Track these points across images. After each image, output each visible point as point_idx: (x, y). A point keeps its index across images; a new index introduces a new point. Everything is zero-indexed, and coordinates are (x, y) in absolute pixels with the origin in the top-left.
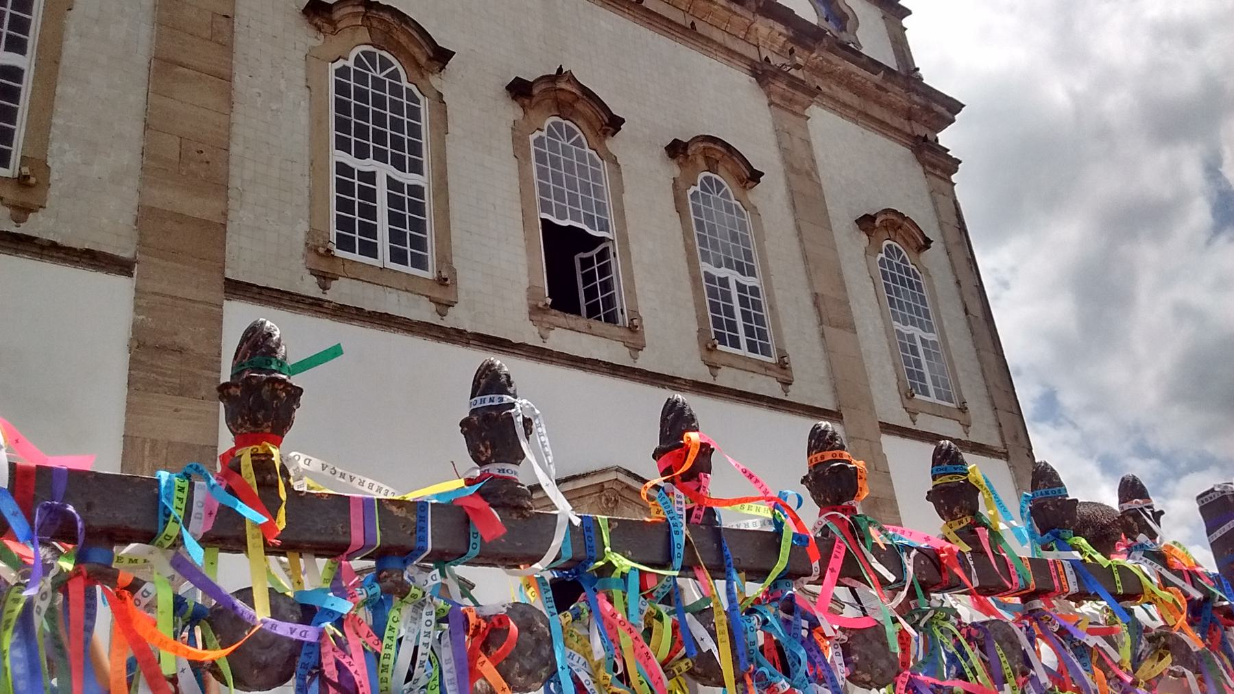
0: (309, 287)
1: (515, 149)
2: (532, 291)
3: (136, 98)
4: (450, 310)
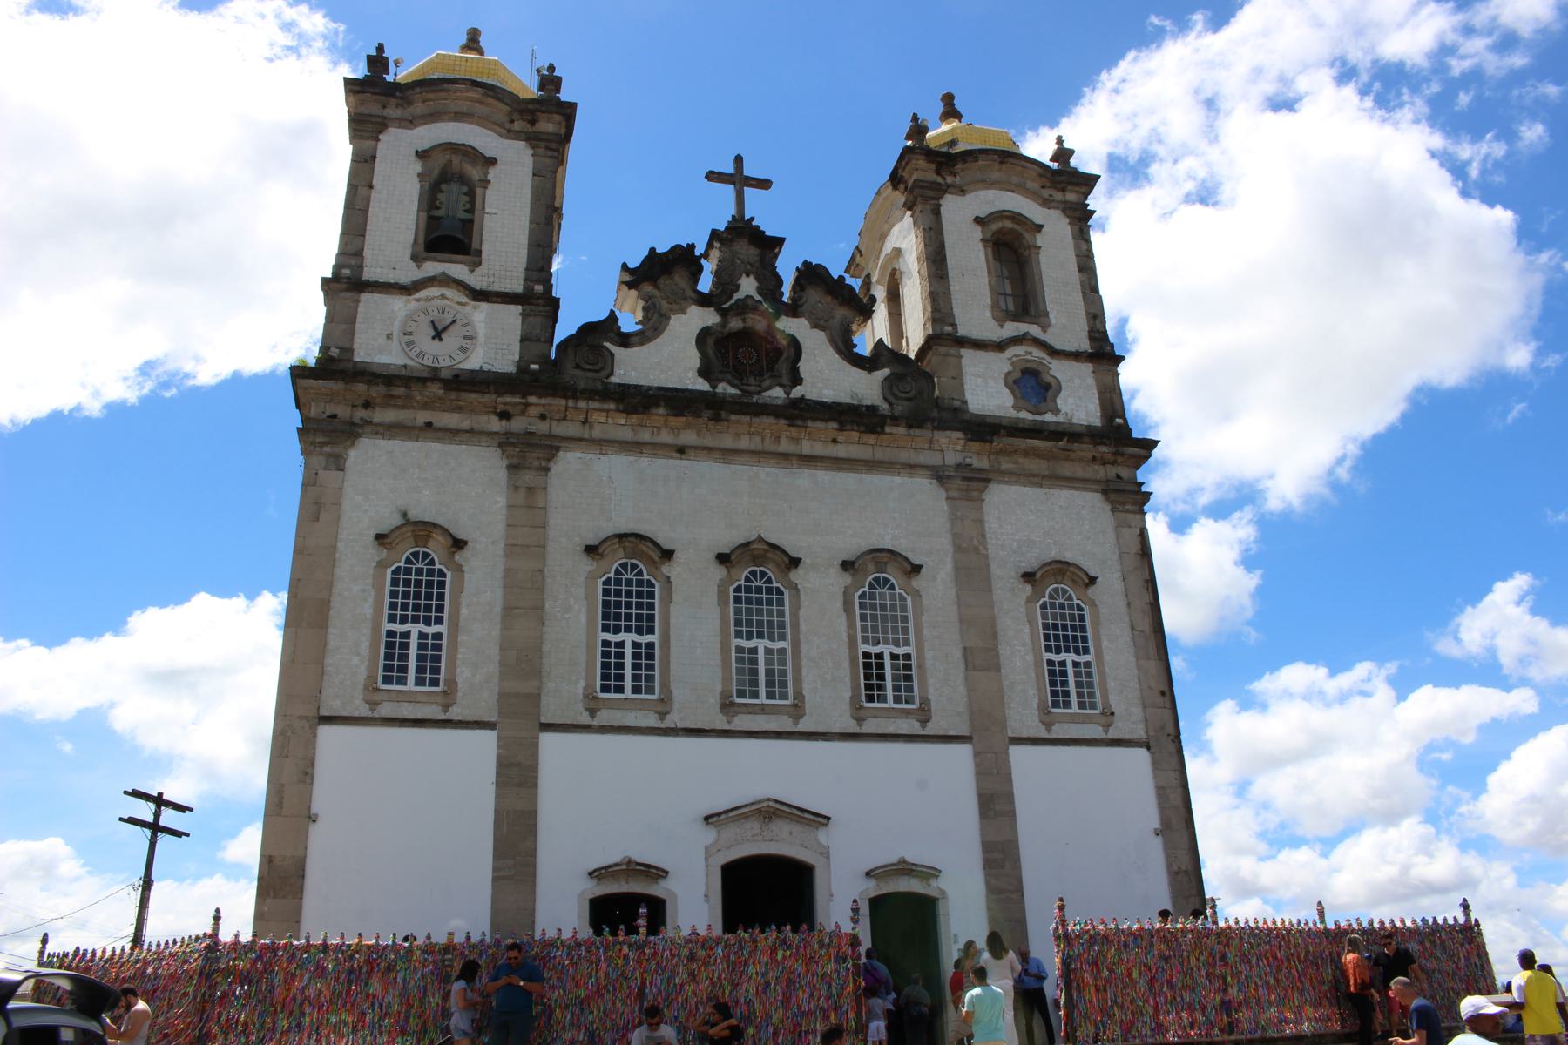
0: (585, 719)
1: (719, 600)
3: (496, 632)
4: (668, 716)
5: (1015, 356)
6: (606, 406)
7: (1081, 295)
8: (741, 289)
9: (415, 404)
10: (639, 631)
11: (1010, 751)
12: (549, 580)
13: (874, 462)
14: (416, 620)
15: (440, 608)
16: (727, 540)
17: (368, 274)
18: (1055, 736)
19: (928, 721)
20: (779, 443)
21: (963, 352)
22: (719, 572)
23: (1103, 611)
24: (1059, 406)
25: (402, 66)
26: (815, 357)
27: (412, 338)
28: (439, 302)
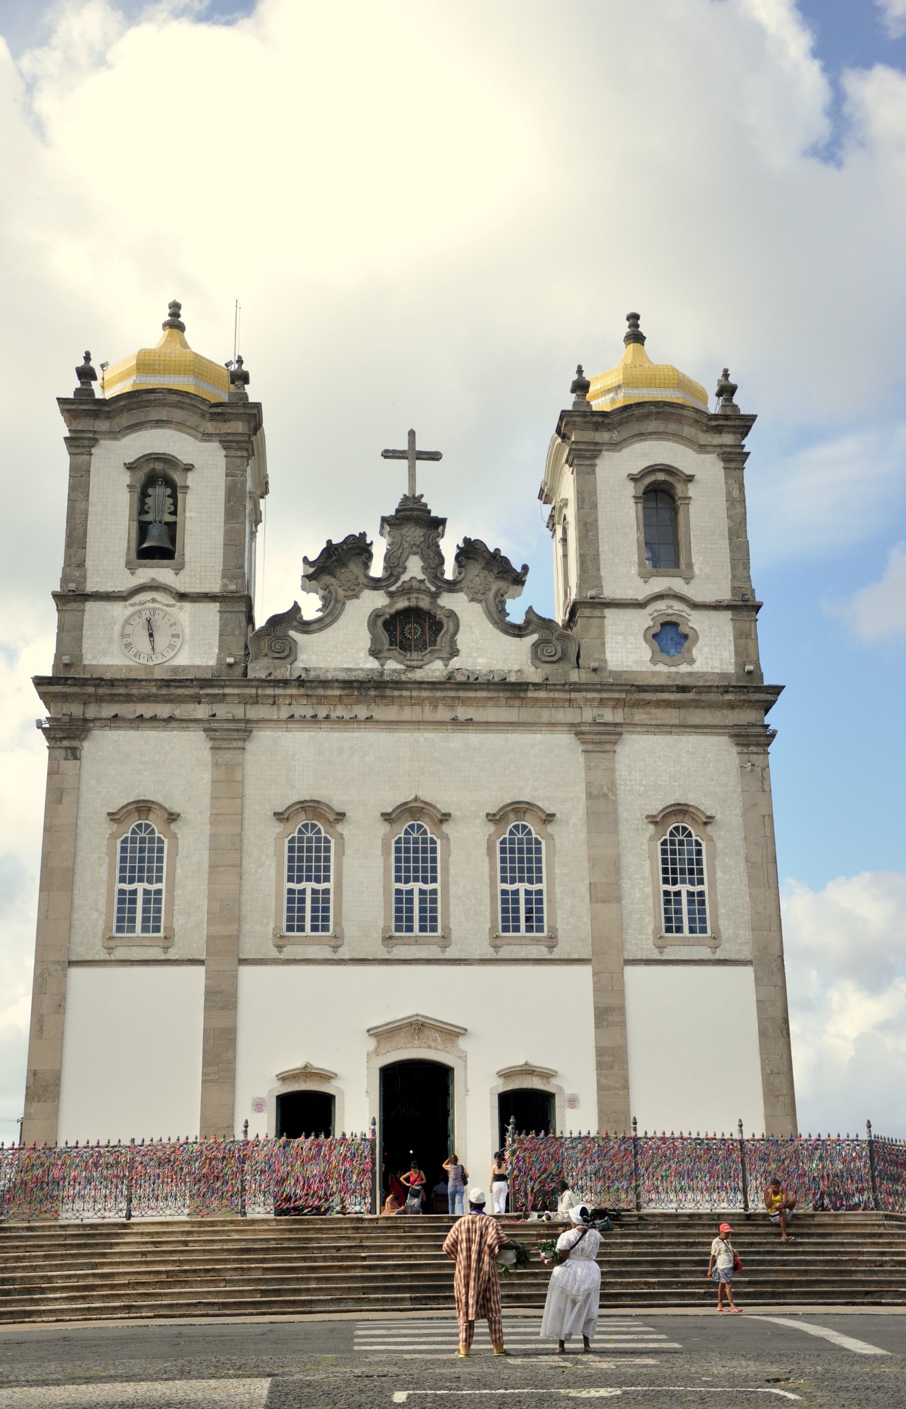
0: (274, 953)
2: (386, 929)
3: (204, 887)
5: (656, 611)
6: (289, 691)
7: (727, 542)
8: (407, 570)
9: (135, 699)
10: (318, 880)
11: (625, 971)
12: (245, 842)
13: (519, 723)
14: (141, 880)
15: (160, 869)
16: (391, 800)
17: (91, 587)
18: (666, 957)
19: (554, 946)
20: (437, 712)
21: (608, 613)
22: (384, 828)
23: (720, 845)
24: (694, 656)
25: (108, 369)
26: (471, 629)
27: (129, 640)
28: (150, 605)
